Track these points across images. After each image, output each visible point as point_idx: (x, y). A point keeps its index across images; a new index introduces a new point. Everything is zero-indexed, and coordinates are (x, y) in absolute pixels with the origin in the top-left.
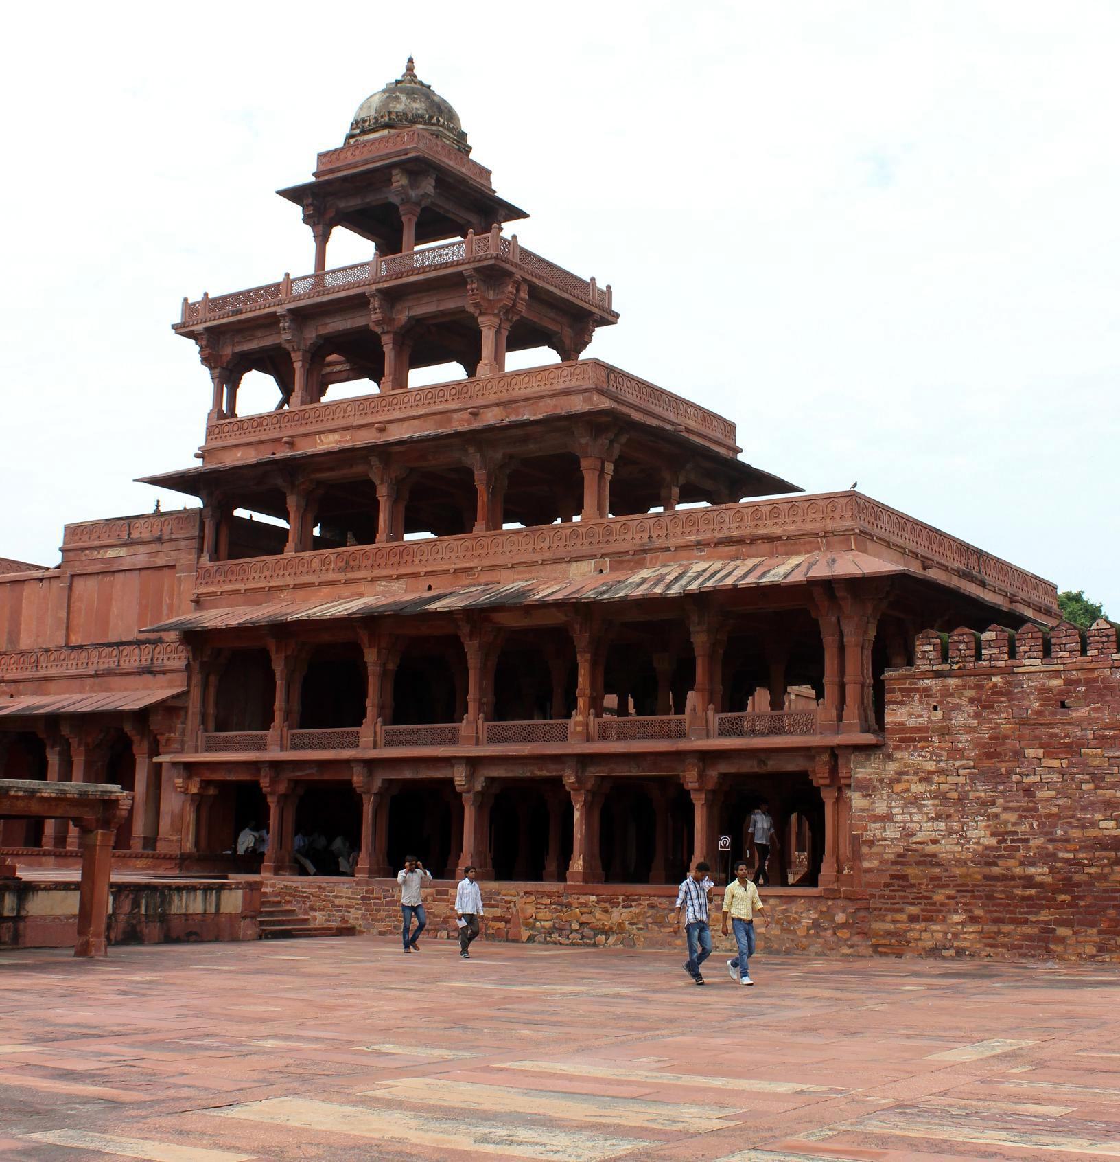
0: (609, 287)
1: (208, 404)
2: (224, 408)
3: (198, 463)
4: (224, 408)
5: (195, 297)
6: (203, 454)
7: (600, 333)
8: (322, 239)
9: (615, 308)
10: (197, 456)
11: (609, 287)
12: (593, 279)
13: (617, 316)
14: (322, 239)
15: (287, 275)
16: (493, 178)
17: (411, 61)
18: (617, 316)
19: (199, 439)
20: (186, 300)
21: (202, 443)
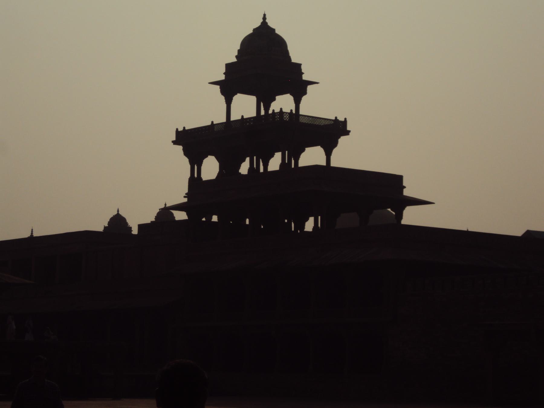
0: (345, 119)
1: (189, 175)
2: (196, 176)
3: (186, 200)
4: (196, 176)
5: (181, 129)
6: (188, 195)
7: (343, 140)
8: (229, 102)
9: (348, 129)
10: (185, 197)
11: (345, 119)
12: (336, 118)
13: (349, 131)
14: (229, 102)
15: (212, 122)
16: (302, 67)
17: (265, 15)
18: (349, 131)
19: (185, 189)
20: (177, 129)
21: (187, 191)
